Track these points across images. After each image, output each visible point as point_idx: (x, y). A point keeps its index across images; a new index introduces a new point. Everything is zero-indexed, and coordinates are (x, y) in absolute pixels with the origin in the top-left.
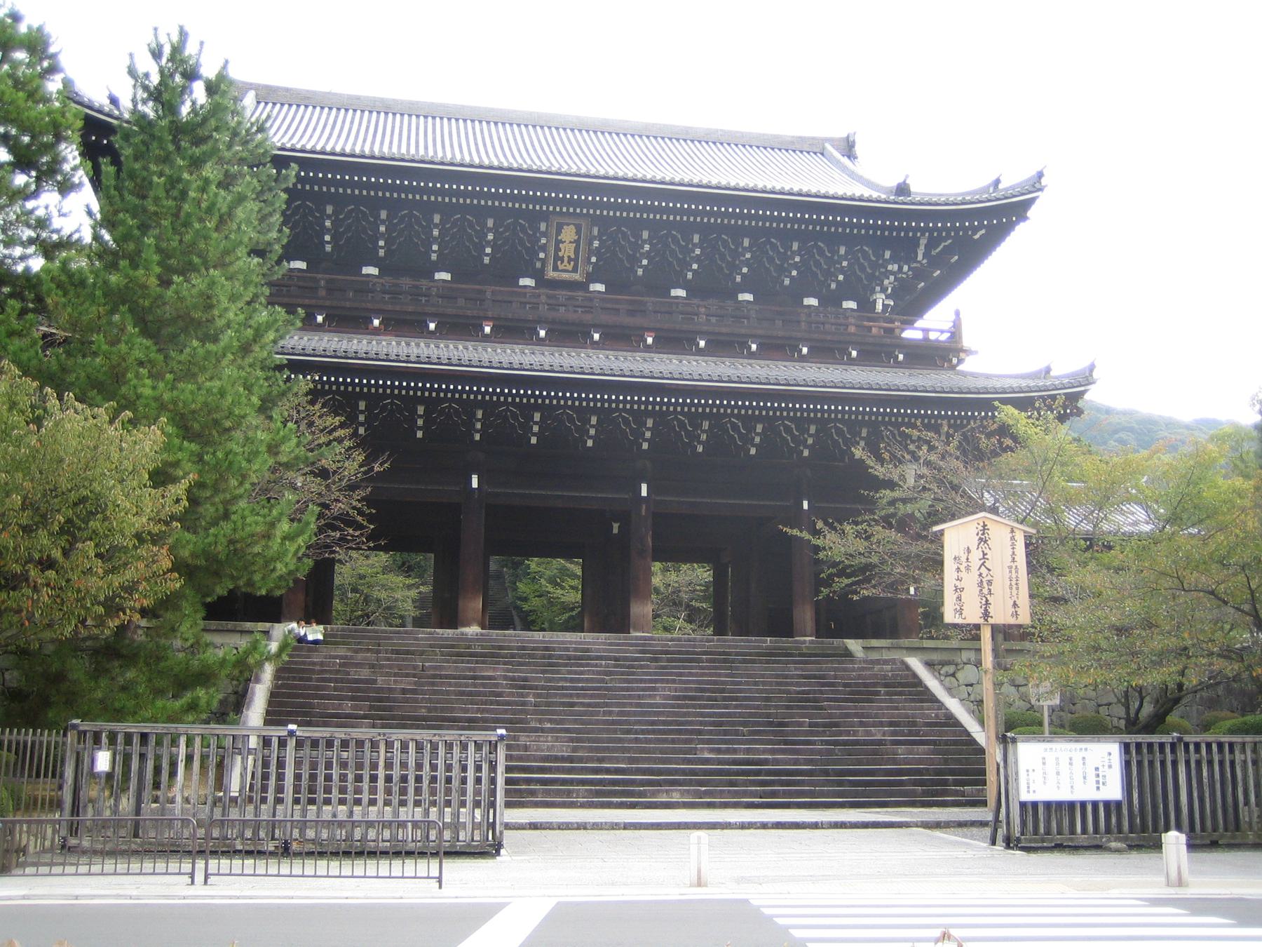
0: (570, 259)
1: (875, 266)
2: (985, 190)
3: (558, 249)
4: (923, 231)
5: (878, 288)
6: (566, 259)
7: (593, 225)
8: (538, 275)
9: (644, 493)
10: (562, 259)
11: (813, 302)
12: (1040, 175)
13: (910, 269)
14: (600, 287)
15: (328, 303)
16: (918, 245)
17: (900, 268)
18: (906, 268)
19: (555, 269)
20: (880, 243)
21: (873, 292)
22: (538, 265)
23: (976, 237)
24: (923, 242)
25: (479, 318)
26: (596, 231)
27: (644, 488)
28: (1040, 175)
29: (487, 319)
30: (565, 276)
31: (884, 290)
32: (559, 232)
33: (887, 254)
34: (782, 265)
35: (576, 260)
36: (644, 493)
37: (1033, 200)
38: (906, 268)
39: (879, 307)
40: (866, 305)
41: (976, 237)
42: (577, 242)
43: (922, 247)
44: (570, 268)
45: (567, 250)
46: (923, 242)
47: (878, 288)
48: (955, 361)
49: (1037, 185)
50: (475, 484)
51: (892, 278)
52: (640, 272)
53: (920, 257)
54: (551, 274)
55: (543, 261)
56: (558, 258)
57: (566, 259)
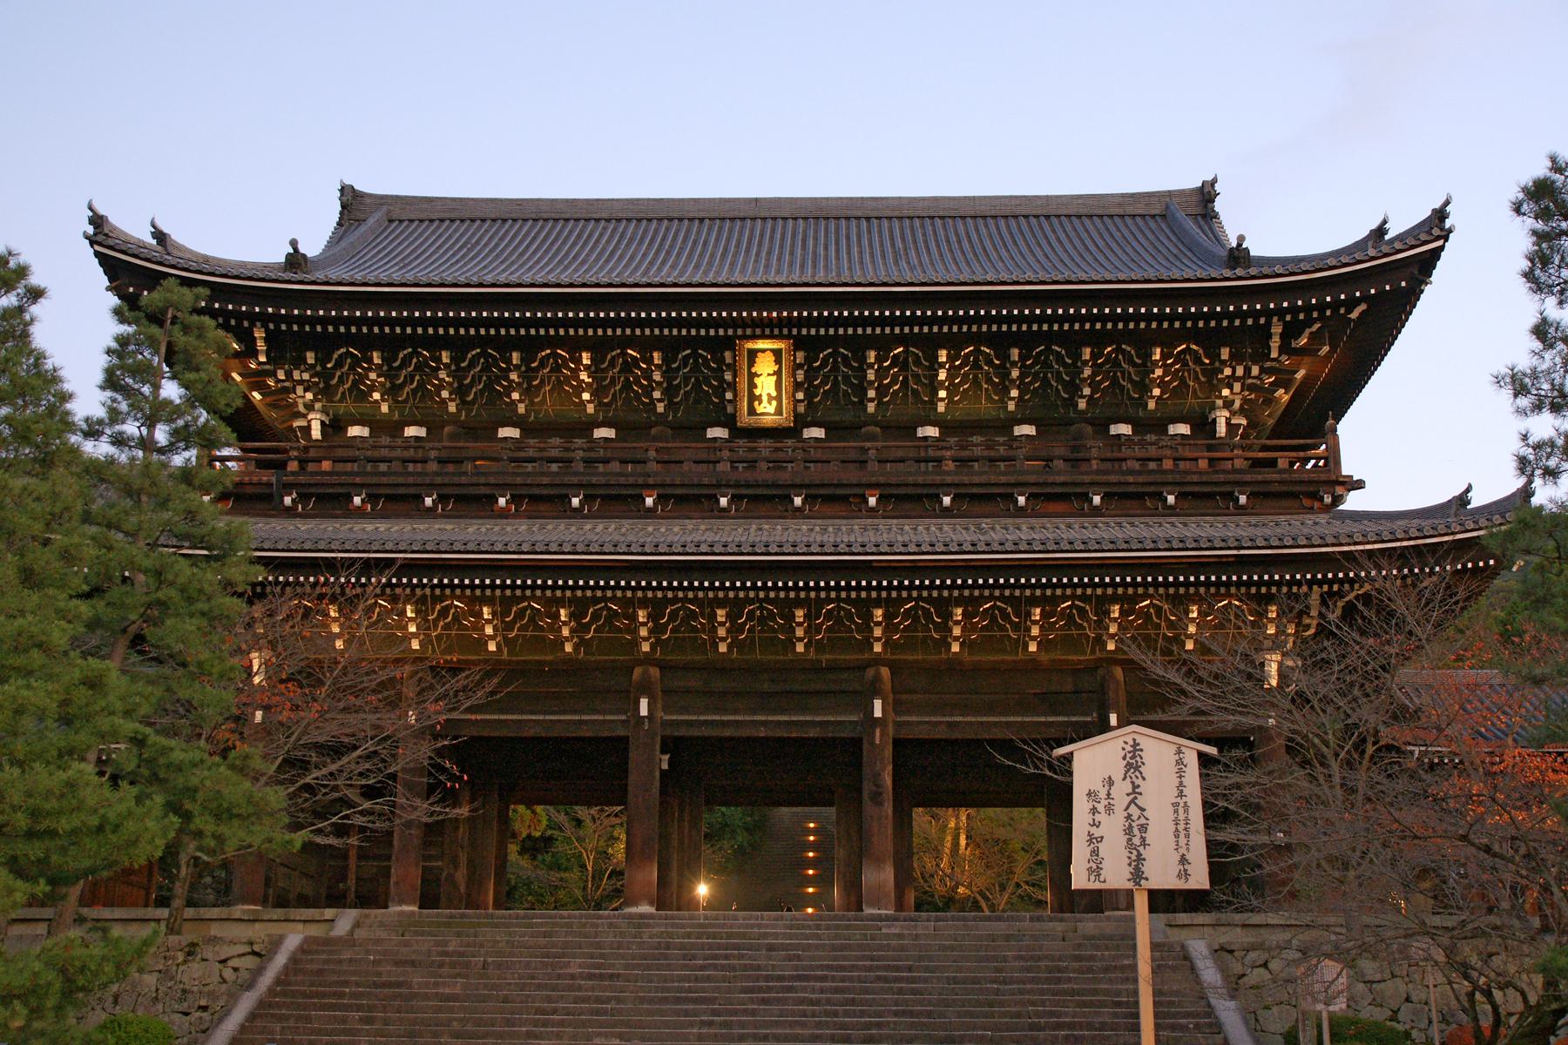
0: (770, 398)
2: (1360, 245)
3: (752, 386)
5: (1219, 402)
6: (765, 398)
8: (730, 422)
9: (878, 713)
10: (759, 398)
11: (1124, 429)
14: (817, 433)
16: (1270, 336)
17: (1248, 370)
18: (1255, 371)
21: (1213, 408)
22: (730, 409)
23: (1354, 315)
24: (1277, 329)
25: (636, 486)
27: (878, 704)
28: (1440, 215)
31: (1228, 404)
33: (1225, 353)
38: (1255, 371)
39: (1222, 429)
40: (1204, 426)
41: (1354, 315)
44: (771, 409)
46: (1277, 329)
47: (1219, 402)
48: (1328, 499)
49: (1436, 232)
50: (644, 711)
51: (1237, 387)
52: (1152, 405)
53: (1274, 355)
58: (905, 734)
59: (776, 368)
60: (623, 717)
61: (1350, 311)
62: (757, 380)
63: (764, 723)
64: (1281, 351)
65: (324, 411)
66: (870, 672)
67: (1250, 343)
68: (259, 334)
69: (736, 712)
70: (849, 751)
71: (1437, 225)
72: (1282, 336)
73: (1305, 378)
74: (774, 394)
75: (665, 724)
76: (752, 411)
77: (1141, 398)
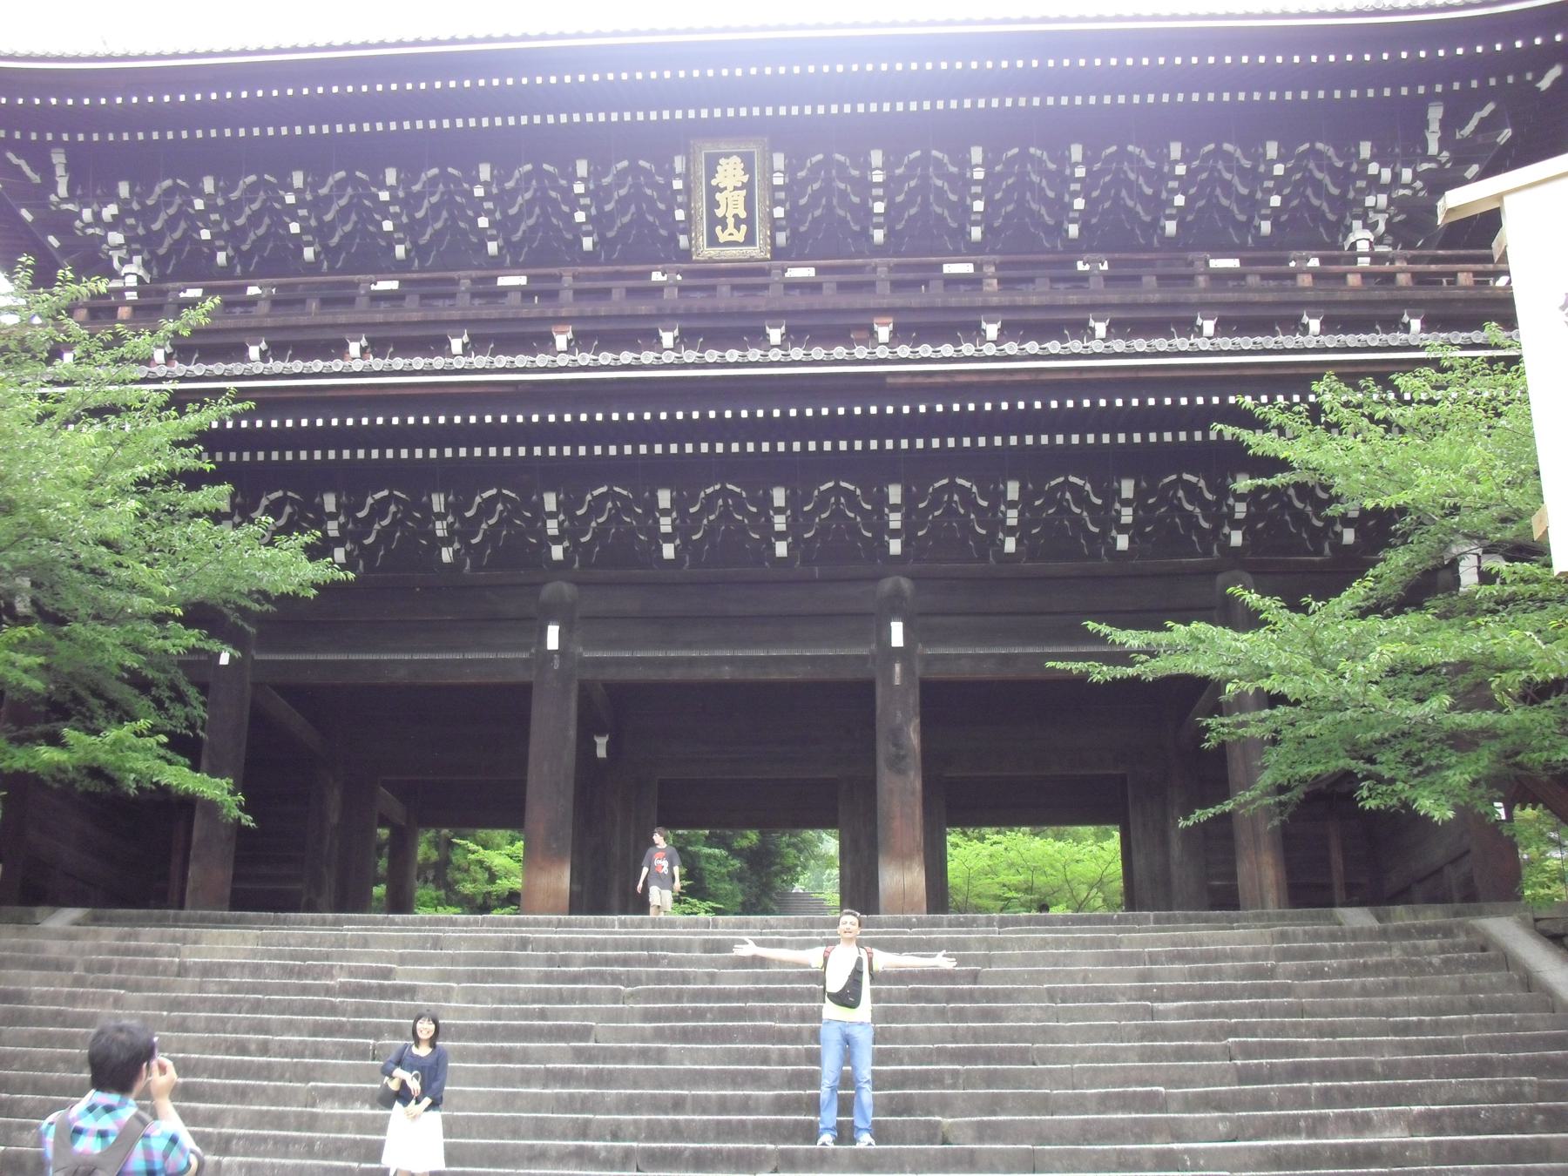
1: (1344, 177)
3: (713, 204)
4: (1431, 97)
6: (731, 221)
7: (775, 148)
8: (686, 255)
13: (1416, 176)
15: (269, 322)
16: (1425, 124)
18: (1407, 175)
21: (1349, 229)
22: (683, 241)
23: (1545, 84)
24: (1435, 113)
26: (779, 160)
32: (711, 172)
34: (1157, 194)
35: (749, 221)
38: (1407, 175)
41: (1545, 84)
42: (748, 187)
43: (1434, 126)
45: (732, 204)
46: (1435, 113)
53: (1433, 148)
54: (706, 252)
56: (715, 222)
57: (731, 221)
58: (938, 673)
59: (745, 179)
60: (525, 655)
61: (1539, 77)
62: (718, 196)
63: (731, 661)
65: (146, 265)
66: (887, 585)
68: (59, 159)
69: (689, 645)
72: (1445, 124)
74: (743, 215)
75: (585, 663)
76: (713, 241)
77: (1251, 219)
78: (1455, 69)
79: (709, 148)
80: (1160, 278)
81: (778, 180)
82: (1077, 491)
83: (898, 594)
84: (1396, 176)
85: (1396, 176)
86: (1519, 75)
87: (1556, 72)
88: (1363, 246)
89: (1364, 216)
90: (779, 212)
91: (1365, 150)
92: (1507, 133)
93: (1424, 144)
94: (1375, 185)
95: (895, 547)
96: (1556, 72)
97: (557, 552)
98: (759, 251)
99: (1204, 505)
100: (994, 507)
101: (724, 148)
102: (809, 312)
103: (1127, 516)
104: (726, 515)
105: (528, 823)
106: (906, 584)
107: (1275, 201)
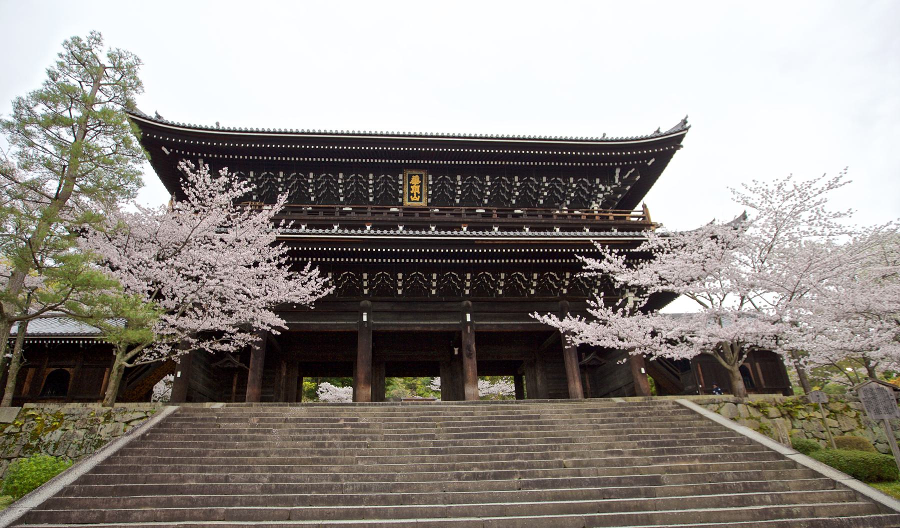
3: (410, 189)
9: (469, 319)
12: (685, 122)
16: (615, 174)
19: (410, 200)
20: (592, 173)
21: (591, 204)
22: (400, 200)
23: (649, 164)
24: (618, 171)
26: (430, 177)
28: (685, 122)
29: (367, 221)
30: (415, 204)
32: (410, 180)
35: (421, 195)
36: (469, 319)
37: (683, 136)
38: (609, 188)
41: (649, 164)
42: (421, 184)
43: (617, 175)
44: (418, 199)
45: (415, 189)
46: (618, 171)
50: (365, 319)
53: (617, 181)
54: (407, 203)
55: (402, 196)
56: (410, 194)
58: (480, 329)
64: (620, 180)
66: (465, 303)
67: (607, 177)
70: (453, 338)
71: (684, 126)
73: (630, 190)
75: (374, 325)
78: (627, 158)
79: (409, 172)
80: (543, 216)
81: (431, 183)
82: (519, 276)
83: (468, 305)
84: (606, 189)
85: (606, 189)
86: (643, 161)
87: (653, 160)
88: (596, 208)
89: (596, 200)
90: (430, 192)
91: (598, 181)
92: (639, 177)
93: (614, 180)
94: (600, 191)
95: (467, 292)
96: (653, 160)
97: (366, 291)
98: (423, 204)
99: (556, 281)
100: (463, 281)
101: (414, 172)
102: (411, 222)
103: (535, 284)
104: (383, 281)
105: (356, 376)
106: (470, 303)
107: (572, 195)
